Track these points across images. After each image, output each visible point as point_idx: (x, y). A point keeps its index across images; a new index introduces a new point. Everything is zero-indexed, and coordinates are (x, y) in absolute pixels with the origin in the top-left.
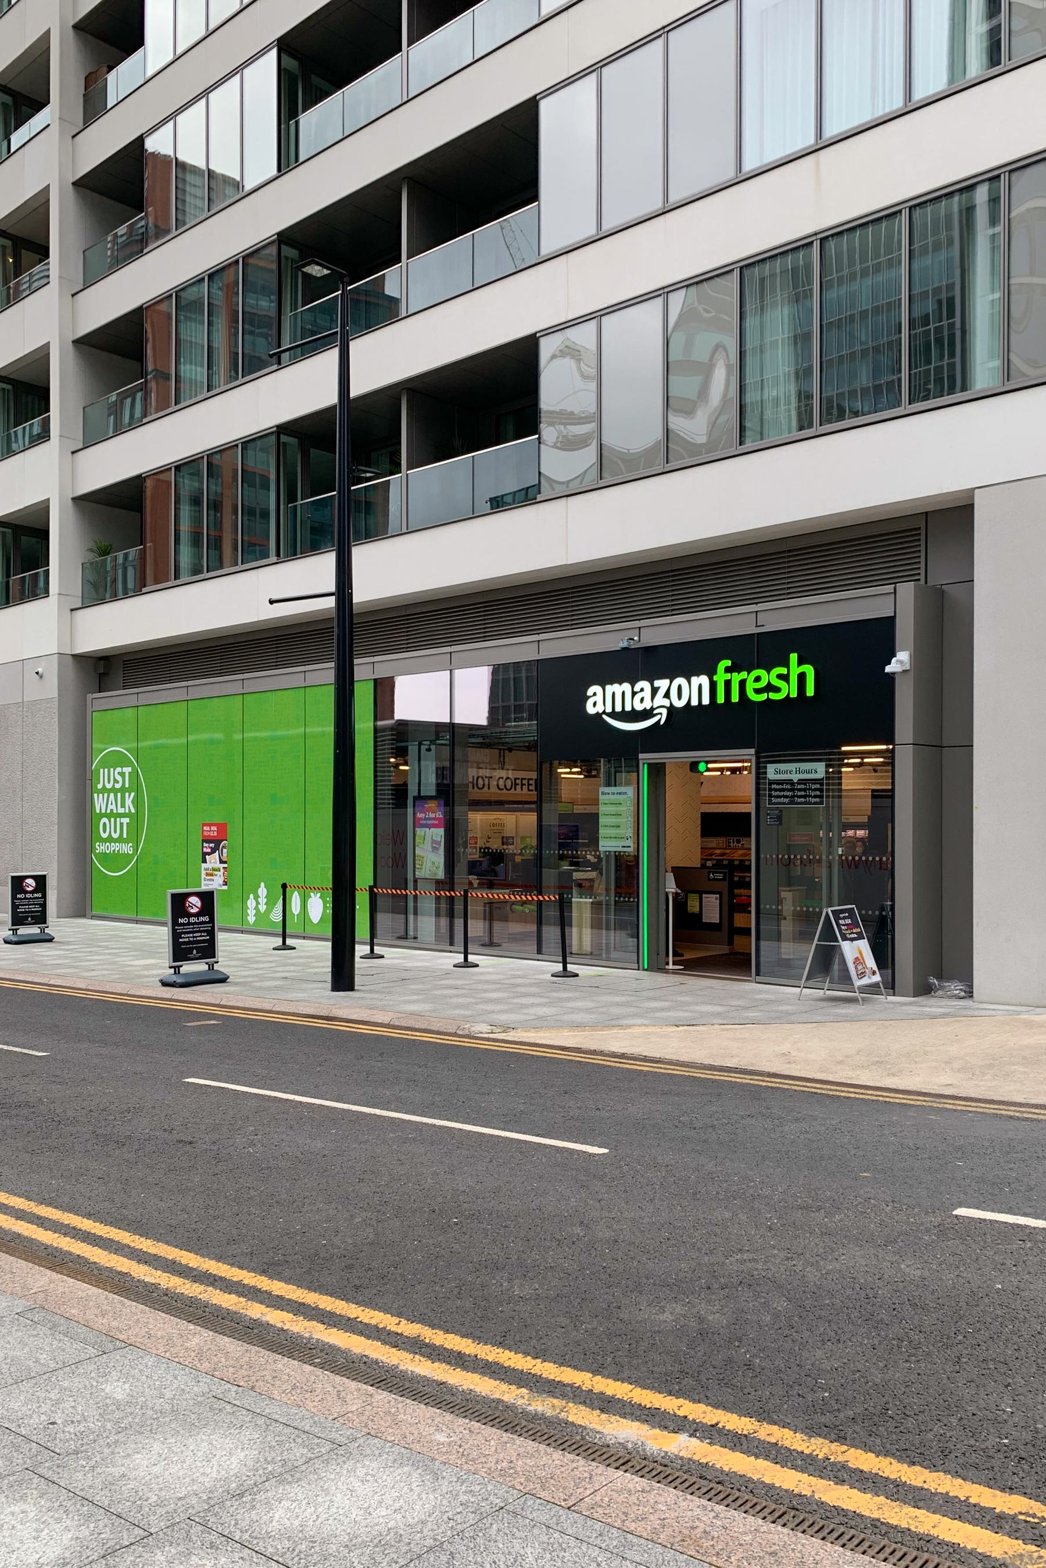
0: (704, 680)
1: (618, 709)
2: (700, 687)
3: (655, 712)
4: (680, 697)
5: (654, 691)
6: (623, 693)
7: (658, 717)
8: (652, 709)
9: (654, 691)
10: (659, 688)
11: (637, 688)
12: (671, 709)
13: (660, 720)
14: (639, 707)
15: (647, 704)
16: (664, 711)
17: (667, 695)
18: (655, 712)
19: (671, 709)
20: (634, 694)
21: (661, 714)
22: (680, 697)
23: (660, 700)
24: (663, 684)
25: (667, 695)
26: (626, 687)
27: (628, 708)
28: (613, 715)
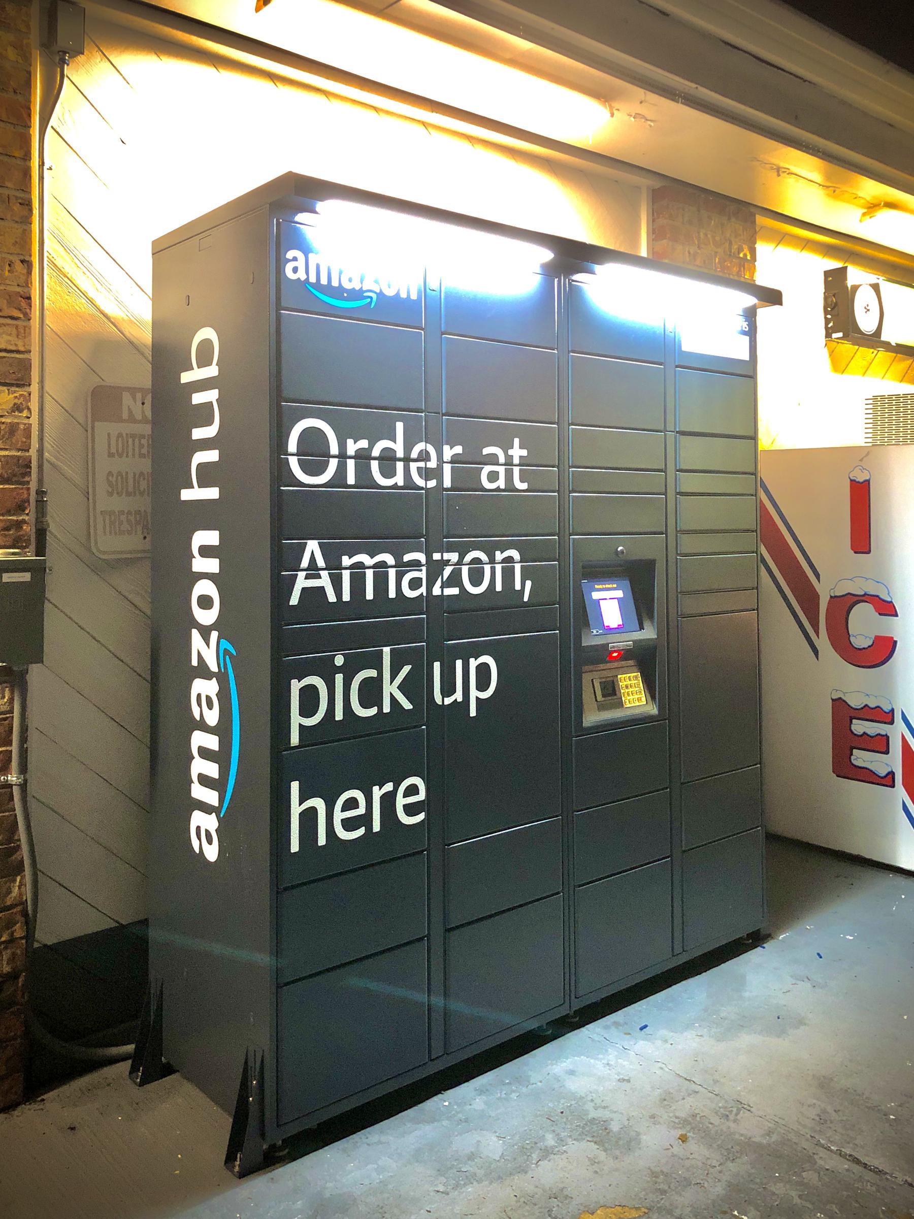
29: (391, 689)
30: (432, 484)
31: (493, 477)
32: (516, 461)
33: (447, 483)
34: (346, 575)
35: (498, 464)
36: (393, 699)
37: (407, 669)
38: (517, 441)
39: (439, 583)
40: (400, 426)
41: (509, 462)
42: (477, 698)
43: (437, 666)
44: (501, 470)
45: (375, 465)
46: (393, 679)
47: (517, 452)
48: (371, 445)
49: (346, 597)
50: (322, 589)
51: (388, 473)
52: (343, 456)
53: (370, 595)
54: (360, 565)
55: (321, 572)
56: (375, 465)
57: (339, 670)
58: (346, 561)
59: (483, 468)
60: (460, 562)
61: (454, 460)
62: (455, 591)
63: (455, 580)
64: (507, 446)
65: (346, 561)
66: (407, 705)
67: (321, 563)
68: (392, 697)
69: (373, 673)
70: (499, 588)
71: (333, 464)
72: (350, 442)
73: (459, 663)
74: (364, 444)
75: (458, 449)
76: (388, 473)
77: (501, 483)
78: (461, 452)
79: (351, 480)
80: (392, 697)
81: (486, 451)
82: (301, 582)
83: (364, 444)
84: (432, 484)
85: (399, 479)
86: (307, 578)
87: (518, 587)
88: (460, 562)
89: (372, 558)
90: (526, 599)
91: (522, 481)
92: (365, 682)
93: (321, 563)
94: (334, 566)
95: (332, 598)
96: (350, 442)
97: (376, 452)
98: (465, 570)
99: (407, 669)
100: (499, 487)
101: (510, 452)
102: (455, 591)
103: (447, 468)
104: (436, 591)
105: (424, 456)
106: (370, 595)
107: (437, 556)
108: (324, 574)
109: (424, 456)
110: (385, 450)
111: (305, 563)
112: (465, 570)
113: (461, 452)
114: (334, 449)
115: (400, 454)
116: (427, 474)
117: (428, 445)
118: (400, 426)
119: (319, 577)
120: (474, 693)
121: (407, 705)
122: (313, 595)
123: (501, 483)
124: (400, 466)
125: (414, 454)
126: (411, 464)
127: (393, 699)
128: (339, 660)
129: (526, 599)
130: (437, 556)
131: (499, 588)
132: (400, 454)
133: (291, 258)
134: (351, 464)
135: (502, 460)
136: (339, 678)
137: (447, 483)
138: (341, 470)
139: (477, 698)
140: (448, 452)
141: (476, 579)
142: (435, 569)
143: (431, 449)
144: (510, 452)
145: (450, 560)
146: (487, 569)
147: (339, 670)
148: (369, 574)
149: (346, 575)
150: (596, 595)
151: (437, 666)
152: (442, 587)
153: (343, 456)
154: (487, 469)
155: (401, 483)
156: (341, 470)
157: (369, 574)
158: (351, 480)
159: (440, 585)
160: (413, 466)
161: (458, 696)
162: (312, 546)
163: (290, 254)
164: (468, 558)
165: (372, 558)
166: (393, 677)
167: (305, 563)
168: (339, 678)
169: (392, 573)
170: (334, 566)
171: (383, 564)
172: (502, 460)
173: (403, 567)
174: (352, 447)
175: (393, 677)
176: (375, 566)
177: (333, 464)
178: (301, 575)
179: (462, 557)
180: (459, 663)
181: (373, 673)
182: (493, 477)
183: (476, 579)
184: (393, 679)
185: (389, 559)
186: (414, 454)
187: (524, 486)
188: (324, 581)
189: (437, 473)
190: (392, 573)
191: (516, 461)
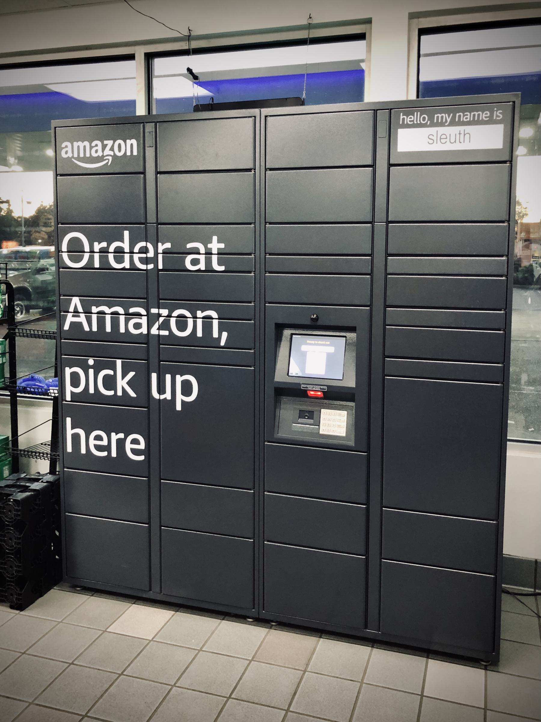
0: (134, 142)
1: (82, 155)
2: (132, 145)
3: (105, 158)
4: (120, 150)
5: (104, 147)
6: (85, 147)
7: (107, 161)
8: (103, 156)
9: (104, 147)
10: (107, 145)
11: (93, 144)
12: (115, 157)
13: (108, 163)
14: (94, 155)
15: (100, 154)
16: (110, 158)
17: (112, 149)
18: (105, 158)
19: (115, 157)
20: (91, 148)
21: (109, 159)
22: (120, 150)
23: (107, 152)
24: (109, 143)
25: (112, 149)
26: (87, 143)
27: (88, 155)
28: (79, 159)
29: (122, 383)
30: (151, 266)
31: (195, 262)
32: (215, 251)
33: (160, 267)
34: (94, 317)
35: (199, 253)
36: (124, 390)
37: (131, 374)
38: (215, 238)
39: (156, 326)
40: (126, 234)
41: (209, 253)
42: (182, 401)
43: (154, 376)
44: (202, 258)
45: (111, 257)
46: (123, 378)
47: (215, 246)
48: (109, 245)
49: (95, 328)
50: (80, 324)
51: (120, 260)
52: (92, 251)
53: (108, 329)
54: (103, 313)
55: (80, 314)
56: (111, 257)
57: (91, 367)
58: (94, 309)
59: (186, 257)
60: (169, 316)
61: (164, 252)
62: (165, 333)
63: (165, 325)
64: (206, 241)
65: (94, 309)
66: (133, 394)
67: (80, 309)
68: (123, 388)
69: (111, 372)
70: (200, 334)
71: (86, 256)
72: (96, 244)
73: (168, 377)
74: (104, 244)
75: (168, 245)
76: (120, 260)
77: (202, 266)
78: (170, 247)
79: (97, 265)
80: (123, 388)
81: (189, 246)
82: (70, 319)
83: (104, 244)
84: (151, 266)
85: (126, 264)
86: (73, 316)
87: (215, 335)
88: (169, 316)
89: (110, 308)
90: (223, 343)
91: (219, 264)
92: (106, 377)
93: (80, 309)
94: (88, 312)
95: (87, 328)
96: (96, 244)
97: (112, 249)
98: (173, 321)
99: (131, 374)
100: (200, 268)
101: (209, 246)
102: (165, 333)
103: (160, 257)
104: (154, 331)
105: (144, 250)
106: (108, 329)
107: (154, 311)
108: (83, 316)
109: (144, 250)
110: (116, 248)
111: (72, 309)
112: (173, 321)
113: (170, 247)
114: (87, 248)
115: (127, 250)
116: (145, 261)
117: (148, 243)
118: (126, 234)
119: (79, 316)
120: (179, 397)
121: (133, 394)
122: (76, 326)
123: (202, 266)
124: (127, 257)
125: (136, 250)
126: (134, 255)
127: (124, 390)
128: (91, 362)
129: (223, 343)
130: (154, 311)
131: (200, 334)
132: (127, 250)
133: (94, 145)
134: (97, 256)
135: (202, 250)
136: (91, 372)
137: (160, 267)
138: (91, 259)
139: (182, 401)
140: (161, 247)
141: (182, 326)
142: (152, 319)
143: (150, 246)
144: (209, 246)
145: (162, 314)
146: (190, 322)
147: (91, 367)
148: (108, 318)
149: (94, 317)
150: (304, 348)
151: (154, 376)
152: (159, 329)
153: (92, 251)
154: (189, 258)
155: (128, 266)
156: (91, 259)
157: (108, 318)
158: (97, 265)
159: (158, 327)
160: (136, 257)
161: (168, 396)
162: (76, 301)
163: (63, 145)
164: (176, 313)
165: (110, 308)
166: (123, 377)
167: (72, 309)
168: (91, 372)
169: (122, 319)
170: (88, 312)
171: (117, 313)
172: (202, 250)
173: (129, 316)
174: (97, 247)
175: (123, 377)
176: (112, 313)
177: (86, 256)
178: (70, 315)
179: (171, 312)
180: (168, 377)
181: (111, 372)
182: (195, 262)
183: (182, 326)
184: (123, 378)
185: (120, 310)
186: (136, 250)
187: (222, 268)
188: (82, 319)
189: (155, 260)
190: (122, 319)
191: (215, 251)
